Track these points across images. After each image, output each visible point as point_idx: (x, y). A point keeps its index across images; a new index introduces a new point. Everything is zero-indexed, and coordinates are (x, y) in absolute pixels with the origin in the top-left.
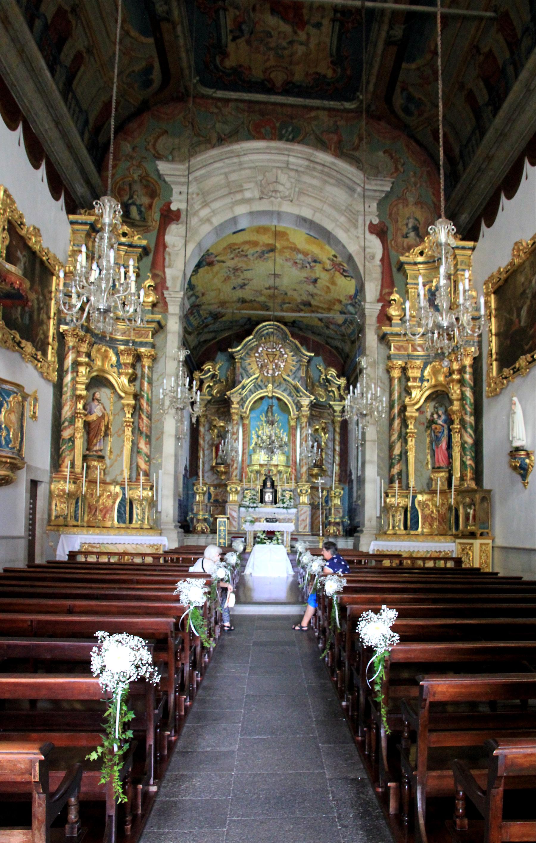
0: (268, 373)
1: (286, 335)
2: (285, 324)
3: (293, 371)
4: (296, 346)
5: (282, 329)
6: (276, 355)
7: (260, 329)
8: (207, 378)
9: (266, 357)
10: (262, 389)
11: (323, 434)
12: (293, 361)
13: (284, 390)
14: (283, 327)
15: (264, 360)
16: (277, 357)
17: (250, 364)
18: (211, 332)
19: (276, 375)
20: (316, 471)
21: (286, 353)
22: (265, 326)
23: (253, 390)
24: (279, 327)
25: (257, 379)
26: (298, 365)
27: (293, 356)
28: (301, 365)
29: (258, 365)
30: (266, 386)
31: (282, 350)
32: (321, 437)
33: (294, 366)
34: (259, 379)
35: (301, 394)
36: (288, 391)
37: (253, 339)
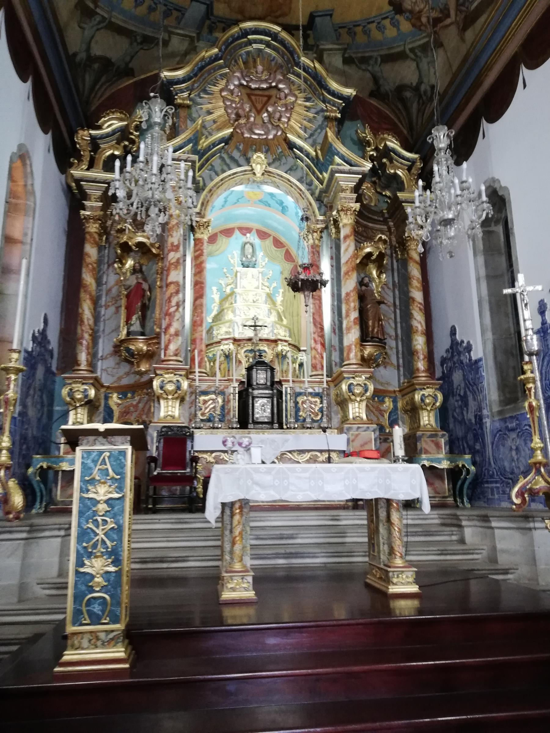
0: (252, 132)
1: (292, 52)
2: (290, 29)
3: (309, 132)
4: (315, 76)
5: (282, 42)
6: (269, 97)
7: (235, 39)
8: (108, 135)
9: (245, 98)
10: (240, 166)
11: (374, 273)
12: (308, 109)
13: (291, 170)
14: (284, 35)
15: (242, 108)
16: (273, 100)
17: (209, 113)
18: (120, 30)
19: (271, 137)
20: (368, 350)
21: (292, 93)
22: (245, 33)
23: (218, 168)
24: (274, 36)
25: (226, 141)
26: (320, 118)
27: (307, 99)
28: (327, 118)
29: (228, 114)
30: (248, 161)
31: (281, 86)
32: (371, 280)
33: (310, 121)
34: (232, 143)
35: (337, 159)
36: (299, 174)
37: (216, 58)
